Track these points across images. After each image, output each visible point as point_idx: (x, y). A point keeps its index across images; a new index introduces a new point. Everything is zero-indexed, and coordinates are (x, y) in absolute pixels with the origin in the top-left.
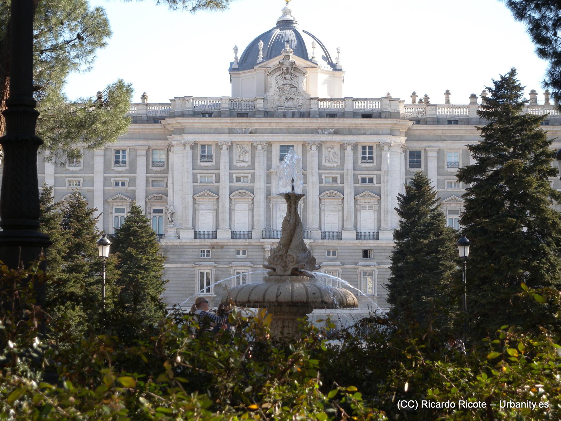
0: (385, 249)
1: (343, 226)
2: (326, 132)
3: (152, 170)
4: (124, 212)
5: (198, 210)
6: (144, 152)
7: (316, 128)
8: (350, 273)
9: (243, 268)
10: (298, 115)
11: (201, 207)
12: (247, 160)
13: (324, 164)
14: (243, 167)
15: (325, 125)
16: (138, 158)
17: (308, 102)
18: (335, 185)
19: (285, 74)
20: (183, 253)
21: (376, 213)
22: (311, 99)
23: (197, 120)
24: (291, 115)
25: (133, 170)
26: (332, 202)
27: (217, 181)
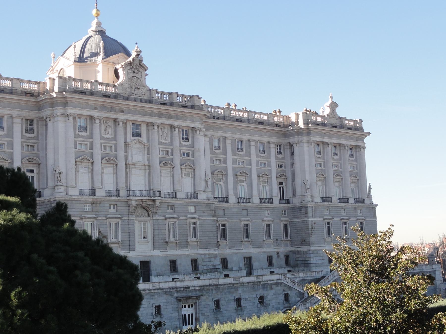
0: (202, 206)
1: (173, 188)
3: (25, 136)
5: (78, 171)
6: (19, 121)
9: (115, 220)
10: (143, 101)
11: (80, 169)
12: (110, 133)
13: (160, 140)
16: (14, 125)
17: (149, 91)
19: (134, 69)
21: (192, 180)
22: (150, 90)
23: (77, 96)
24: (139, 101)
26: (166, 170)
27: (91, 148)
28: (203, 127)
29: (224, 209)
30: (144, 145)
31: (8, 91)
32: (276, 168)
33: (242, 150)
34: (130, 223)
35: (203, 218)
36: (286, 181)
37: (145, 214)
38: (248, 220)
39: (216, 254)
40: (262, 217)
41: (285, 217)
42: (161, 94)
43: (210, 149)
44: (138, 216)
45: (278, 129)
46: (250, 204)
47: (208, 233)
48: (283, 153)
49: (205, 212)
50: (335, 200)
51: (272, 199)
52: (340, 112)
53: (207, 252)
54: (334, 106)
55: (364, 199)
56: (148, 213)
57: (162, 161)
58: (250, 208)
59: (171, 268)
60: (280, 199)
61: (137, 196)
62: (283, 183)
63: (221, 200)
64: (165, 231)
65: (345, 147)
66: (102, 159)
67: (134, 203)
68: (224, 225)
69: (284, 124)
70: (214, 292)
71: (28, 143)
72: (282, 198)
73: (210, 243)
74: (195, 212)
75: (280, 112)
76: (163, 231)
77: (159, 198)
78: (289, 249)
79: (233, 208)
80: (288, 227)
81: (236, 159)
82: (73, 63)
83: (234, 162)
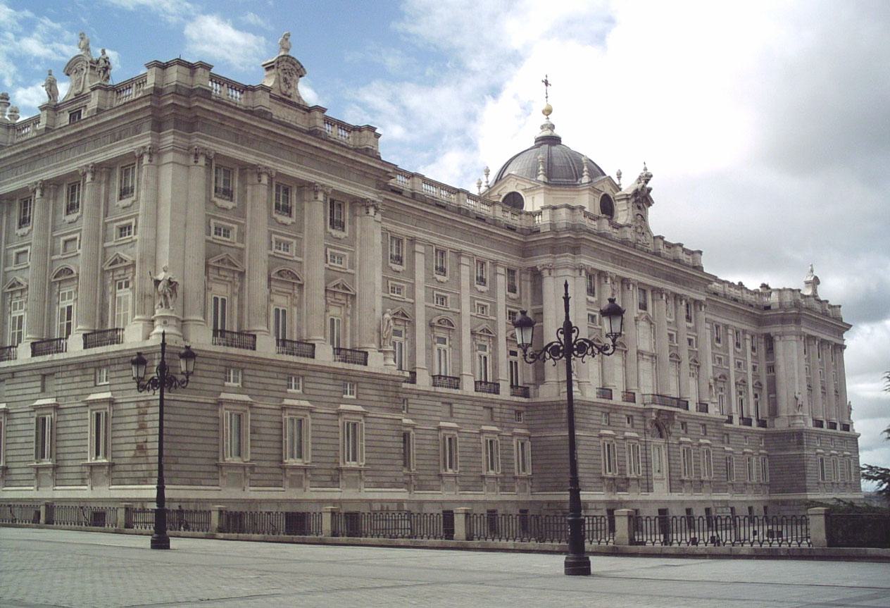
4: (485, 351)
16: (498, 277)
22: (654, 238)
25: (492, 293)
49: (716, 434)
78: (768, 498)
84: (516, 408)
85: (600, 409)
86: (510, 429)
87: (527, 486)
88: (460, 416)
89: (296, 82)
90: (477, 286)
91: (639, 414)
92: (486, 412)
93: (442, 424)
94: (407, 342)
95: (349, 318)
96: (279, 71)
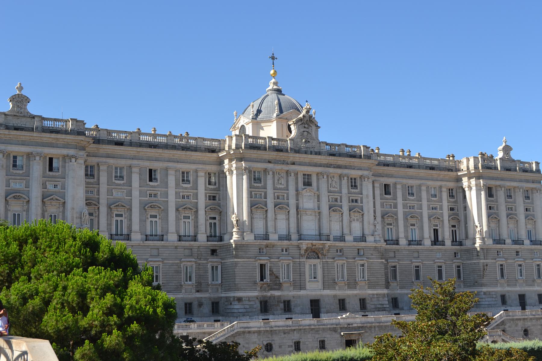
0: (370, 249)
1: (343, 232)
2: (332, 167)
4: (189, 219)
6: (203, 174)
7: (327, 163)
8: (352, 265)
9: (287, 262)
10: (313, 153)
11: (255, 216)
12: (283, 183)
13: (330, 189)
14: (282, 188)
15: (332, 161)
16: (199, 178)
17: (318, 145)
18: (336, 203)
19: (305, 124)
20: (247, 251)
21: (361, 224)
22: (320, 143)
23: (252, 151)
24: (309, 153)
26: (335, 215)
27: (266, 198)
28: (371, 174)
29: (394, 252)
30: (315, 194)
31: (193, 149)
32: (449, 211)
33: (413, 194)
34: (301, 265)
35: (371, 260)
36: (459, 224)
37: (315, 256)
38: (420, 262)
39: (384, 294)
40: (433, 259)
41: (458, 259)
42: (331, 146)
43: (380, 194)
44: (309, 258)
45: (451, 173)
46: (420, 246)
47: (376, 274)
48: (455, 196)
50: (508, 241)
51: (444, 241)
52: (515, 155)
53: (375, 292)
54: (507, 149)
55: (541, 241)
56: (318, 256)
57: (332, 208)
58: (421, 250)
59: (340, 305)
60: (453, 241)
61: (307, 240)
62: (455, 226)
63: (392, 242)
64: (334, 272)
65: (520, 189)
66: (275, 207)
67: (304, 247)
68: (395, 267)
69: (456, 169)
70: (377, 329)
71: (210, 193)
72: (455, 240)
73: (379, 283)
74: (363, 255)
75: (453, 157)
76: (332, 272)
77: (328, 242)
79: (403, 250)
80: (461, 268)
81: (407, 203)
82: (250, 121)
83: (404, 206)
84: (212, 248)
85: (257, 246)
86: (207, 259)
87: (219, 289)
88: (164, 255)
89: (26, 105)
90: (183, 185)
91: (297, 246)
92: (187, 252)
93: (149, 259)
94: (126, 220)
95: (61, 214)
96: (14, 102)
